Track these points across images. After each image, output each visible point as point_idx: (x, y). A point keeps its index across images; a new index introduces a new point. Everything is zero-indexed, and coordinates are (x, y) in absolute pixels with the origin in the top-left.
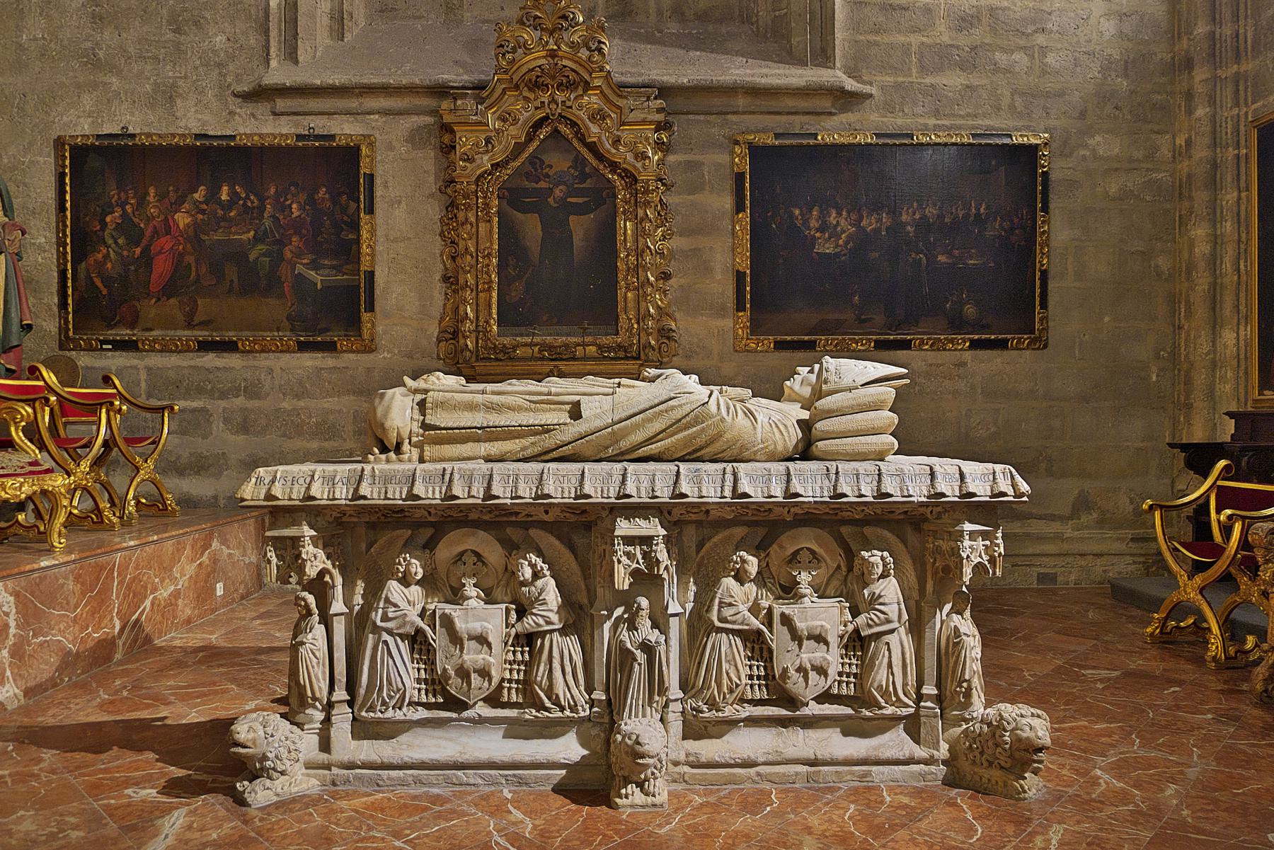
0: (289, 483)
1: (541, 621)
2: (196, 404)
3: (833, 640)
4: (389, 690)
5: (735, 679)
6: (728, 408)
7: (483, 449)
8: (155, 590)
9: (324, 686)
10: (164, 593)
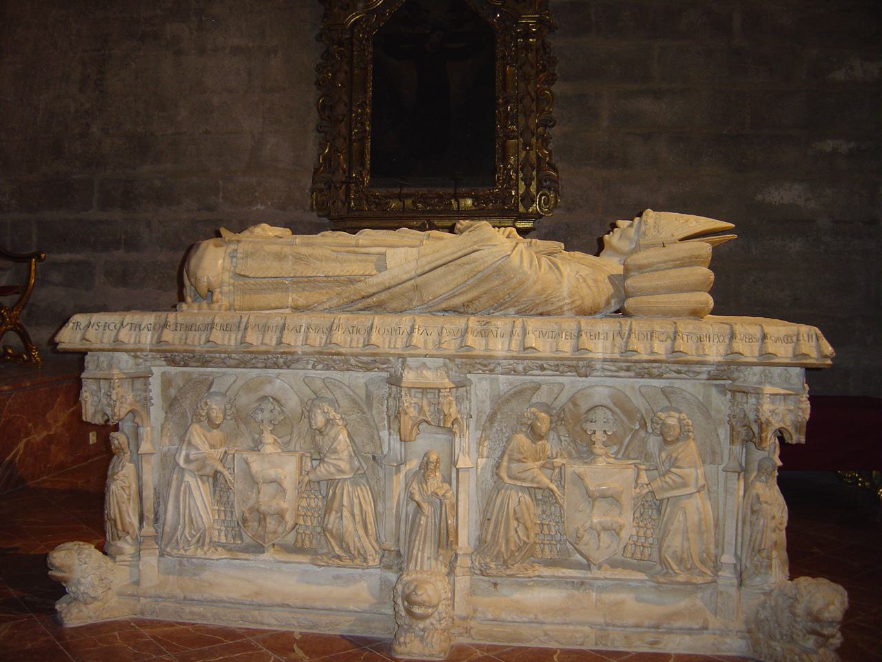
0: (101, 328)
1: (332, 469)
2: (80, 257)
3: (627, 501)
4: (191, 529)
5: (525, 539)
6: (531, 262)
7: (290, 299)
8: (28, 434)
9: (136, 521)
10: (38, 437)
